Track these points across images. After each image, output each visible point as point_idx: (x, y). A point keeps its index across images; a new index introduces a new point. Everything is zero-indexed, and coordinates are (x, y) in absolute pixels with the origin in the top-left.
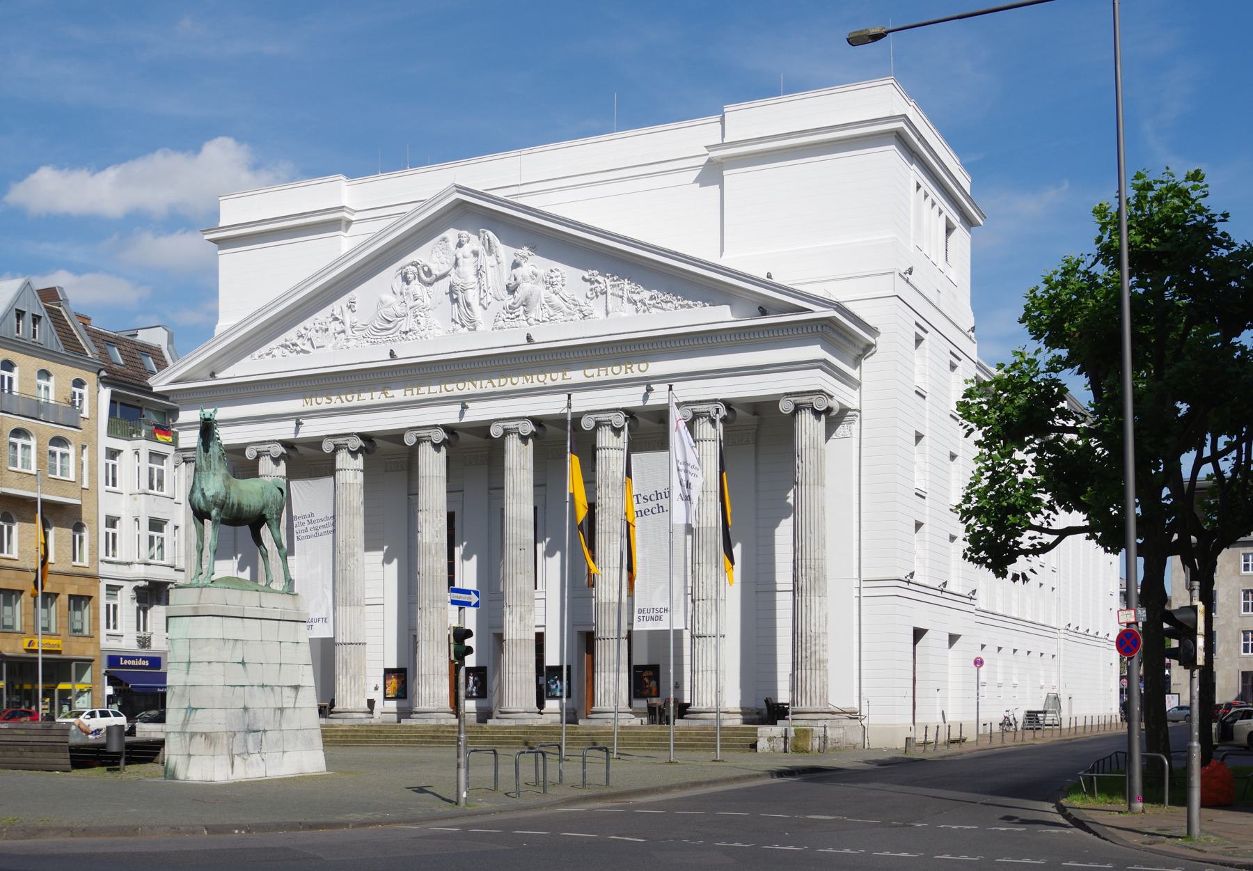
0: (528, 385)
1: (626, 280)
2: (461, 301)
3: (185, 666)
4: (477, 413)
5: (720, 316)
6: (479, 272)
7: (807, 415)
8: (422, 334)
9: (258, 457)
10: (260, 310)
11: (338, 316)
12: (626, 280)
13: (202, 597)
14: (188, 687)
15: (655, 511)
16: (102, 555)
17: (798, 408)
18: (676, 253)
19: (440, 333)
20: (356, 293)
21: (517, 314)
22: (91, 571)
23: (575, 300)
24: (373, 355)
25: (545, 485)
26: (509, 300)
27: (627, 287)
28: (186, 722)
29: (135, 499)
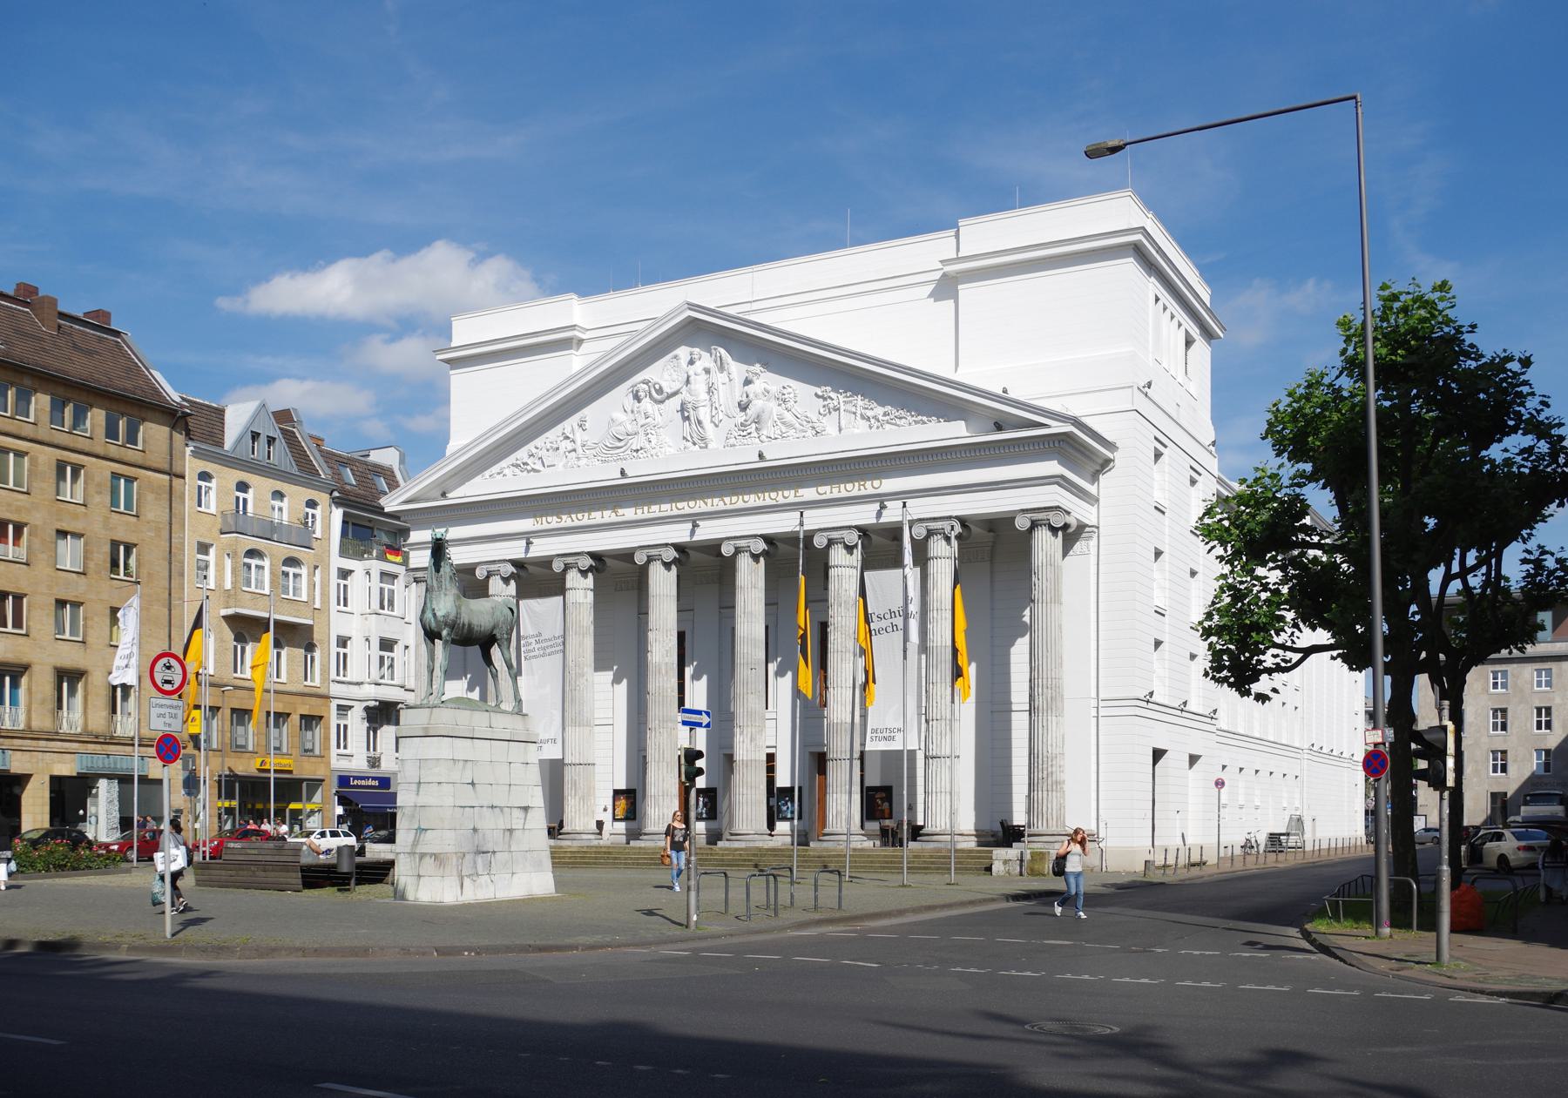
0: (760, 503)
1: (859, 396)
2: (692, 418)
3: (414, 787)
4: (708, 531)
5: (955, 432)
6: (710, 391)
7: (1044, 531)
8: (653, 452)
9: (488, 577)
10: (491, 430)
11: (568, 435)
12: (859, 396)
13: (432, 718)
14: (418, 808)
15: (889, 629)
16: (333, 675)
17: (1034, 525)
18: (910, 369)
19: (672, 451)
20: (587, 412)
21: (749, 431)
22: (322, 691)
23: (807, 417)
24: (603, 474)
25: (777, 604)
26: (741, 417)
27: (860, 403)
28: (415, 843)
29: (366, 619)
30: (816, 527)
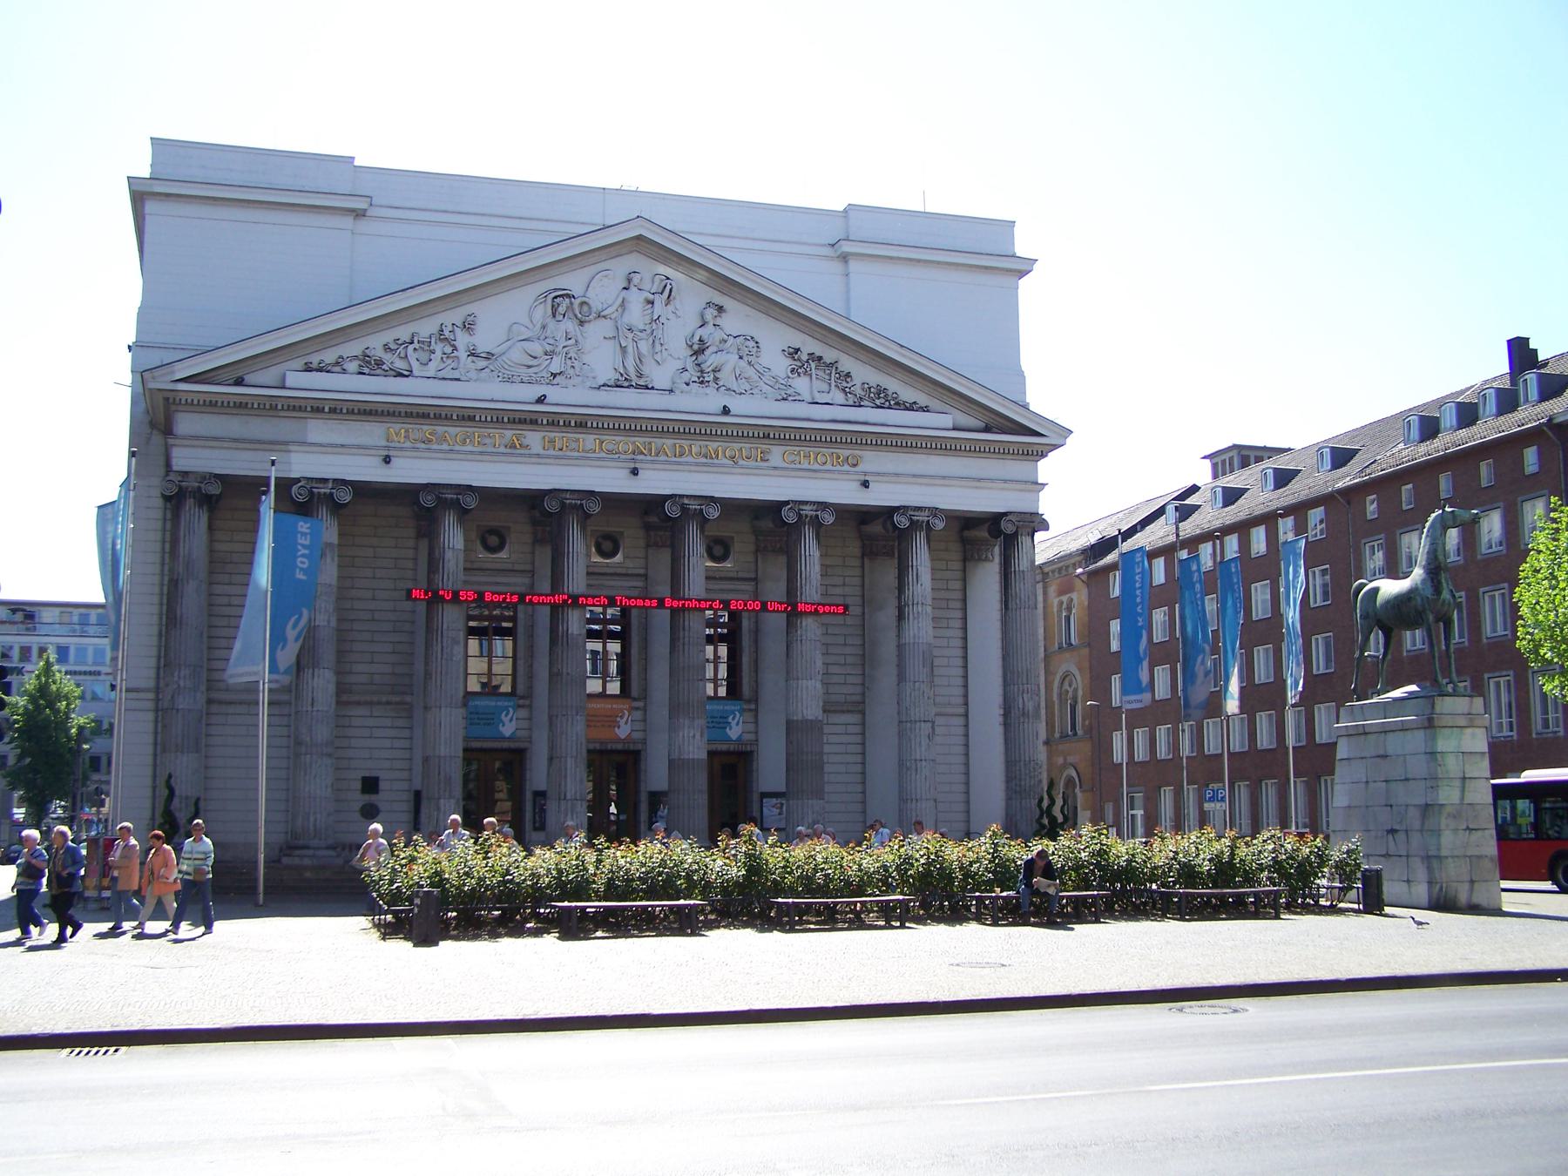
3: (1458, 783)
5: (939, 421)
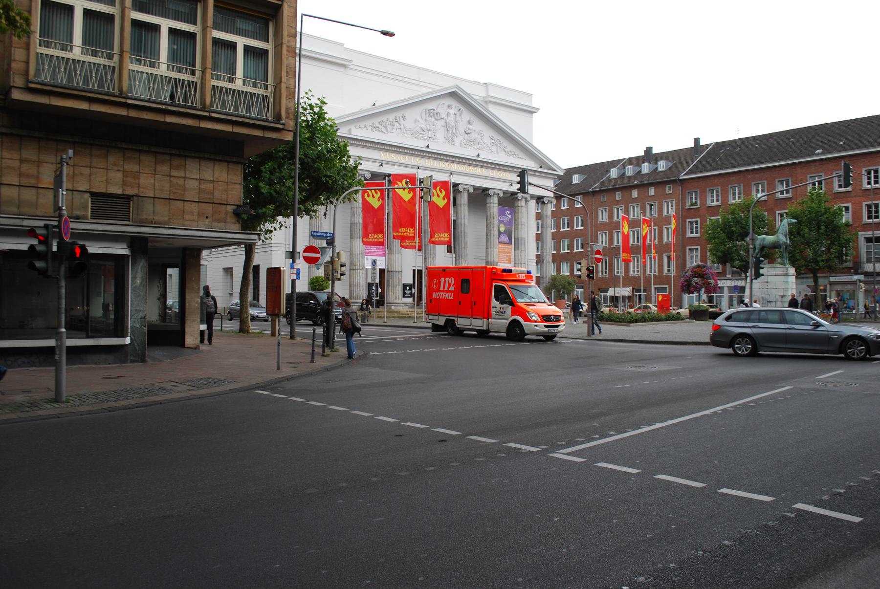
6: (456, 122)
8: (436, 140)
24: (420, 145)
30: (490, 187)
